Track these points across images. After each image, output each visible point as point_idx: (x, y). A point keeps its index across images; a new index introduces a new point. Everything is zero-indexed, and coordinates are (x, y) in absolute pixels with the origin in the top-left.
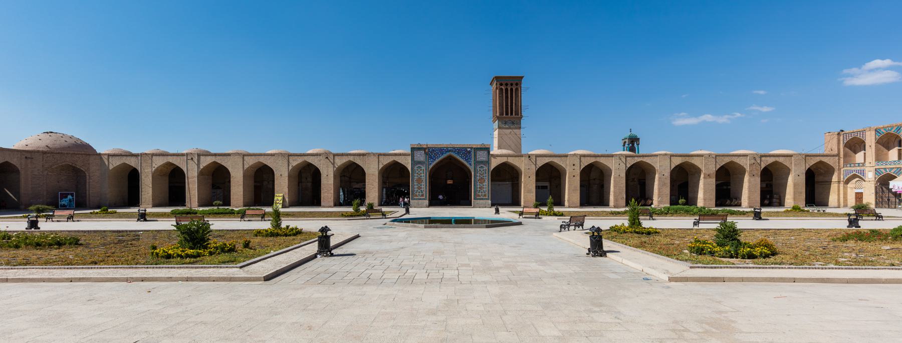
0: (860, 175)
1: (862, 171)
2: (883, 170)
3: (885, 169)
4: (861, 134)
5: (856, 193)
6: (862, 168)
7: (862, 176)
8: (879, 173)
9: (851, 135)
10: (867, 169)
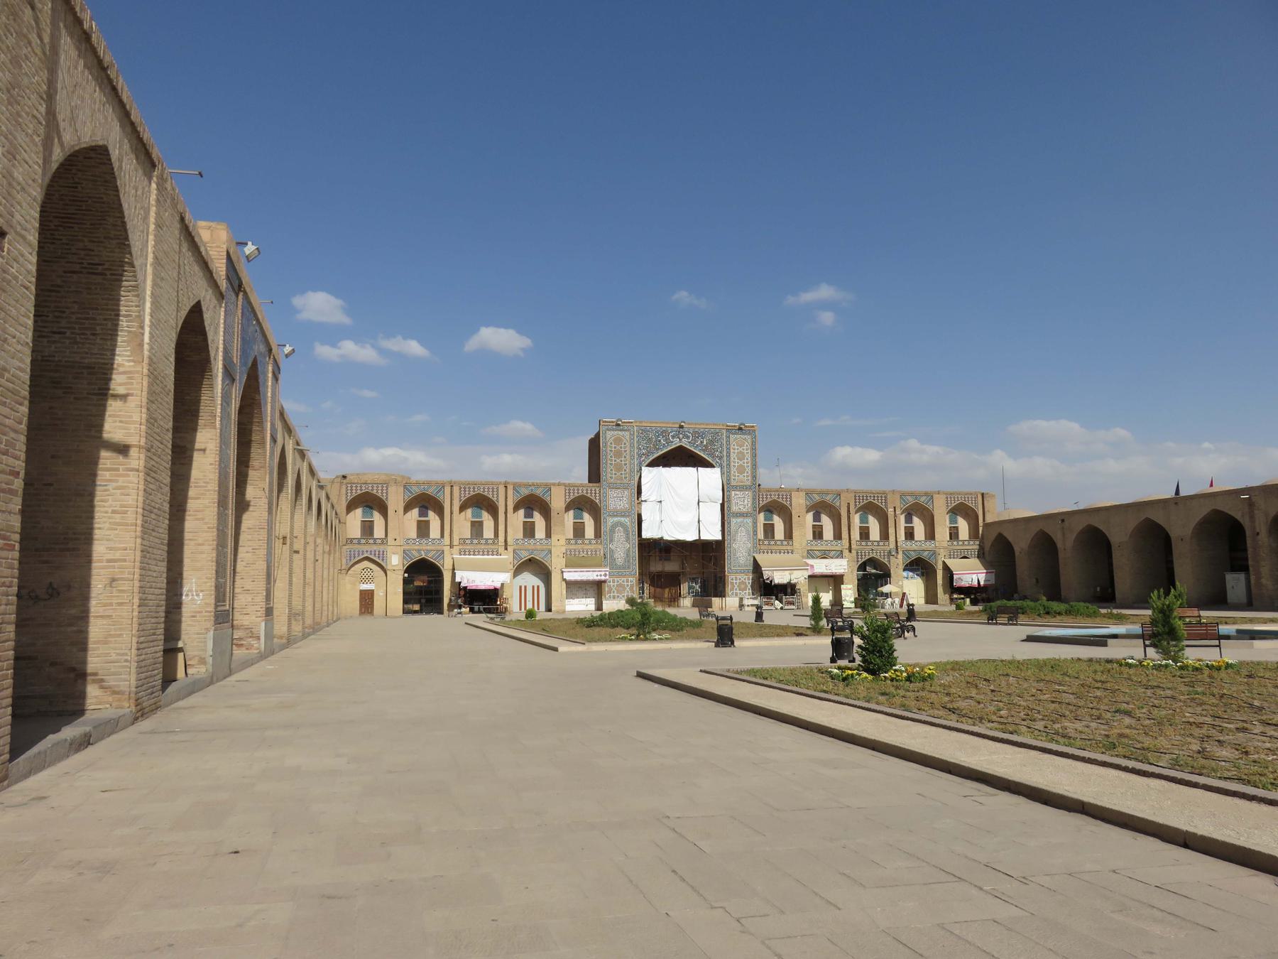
0: (377, 560)
1: (381, 553)
2: (414, 552)
3: (419, 551)
4: (380, 488)
5: (361, 591)
6: (382, 548)
7: (380, 561)
8: (410, 557)
9: (361, 487)
10: (389, 549)
